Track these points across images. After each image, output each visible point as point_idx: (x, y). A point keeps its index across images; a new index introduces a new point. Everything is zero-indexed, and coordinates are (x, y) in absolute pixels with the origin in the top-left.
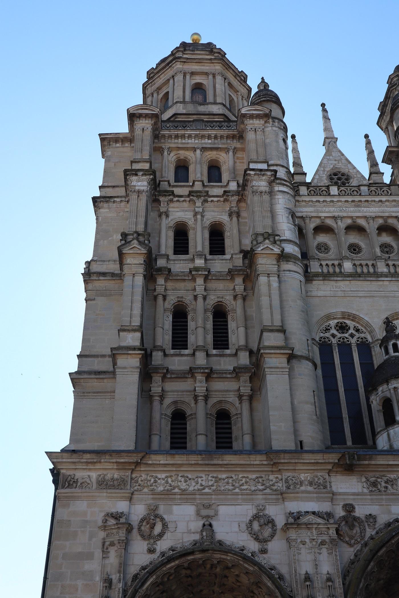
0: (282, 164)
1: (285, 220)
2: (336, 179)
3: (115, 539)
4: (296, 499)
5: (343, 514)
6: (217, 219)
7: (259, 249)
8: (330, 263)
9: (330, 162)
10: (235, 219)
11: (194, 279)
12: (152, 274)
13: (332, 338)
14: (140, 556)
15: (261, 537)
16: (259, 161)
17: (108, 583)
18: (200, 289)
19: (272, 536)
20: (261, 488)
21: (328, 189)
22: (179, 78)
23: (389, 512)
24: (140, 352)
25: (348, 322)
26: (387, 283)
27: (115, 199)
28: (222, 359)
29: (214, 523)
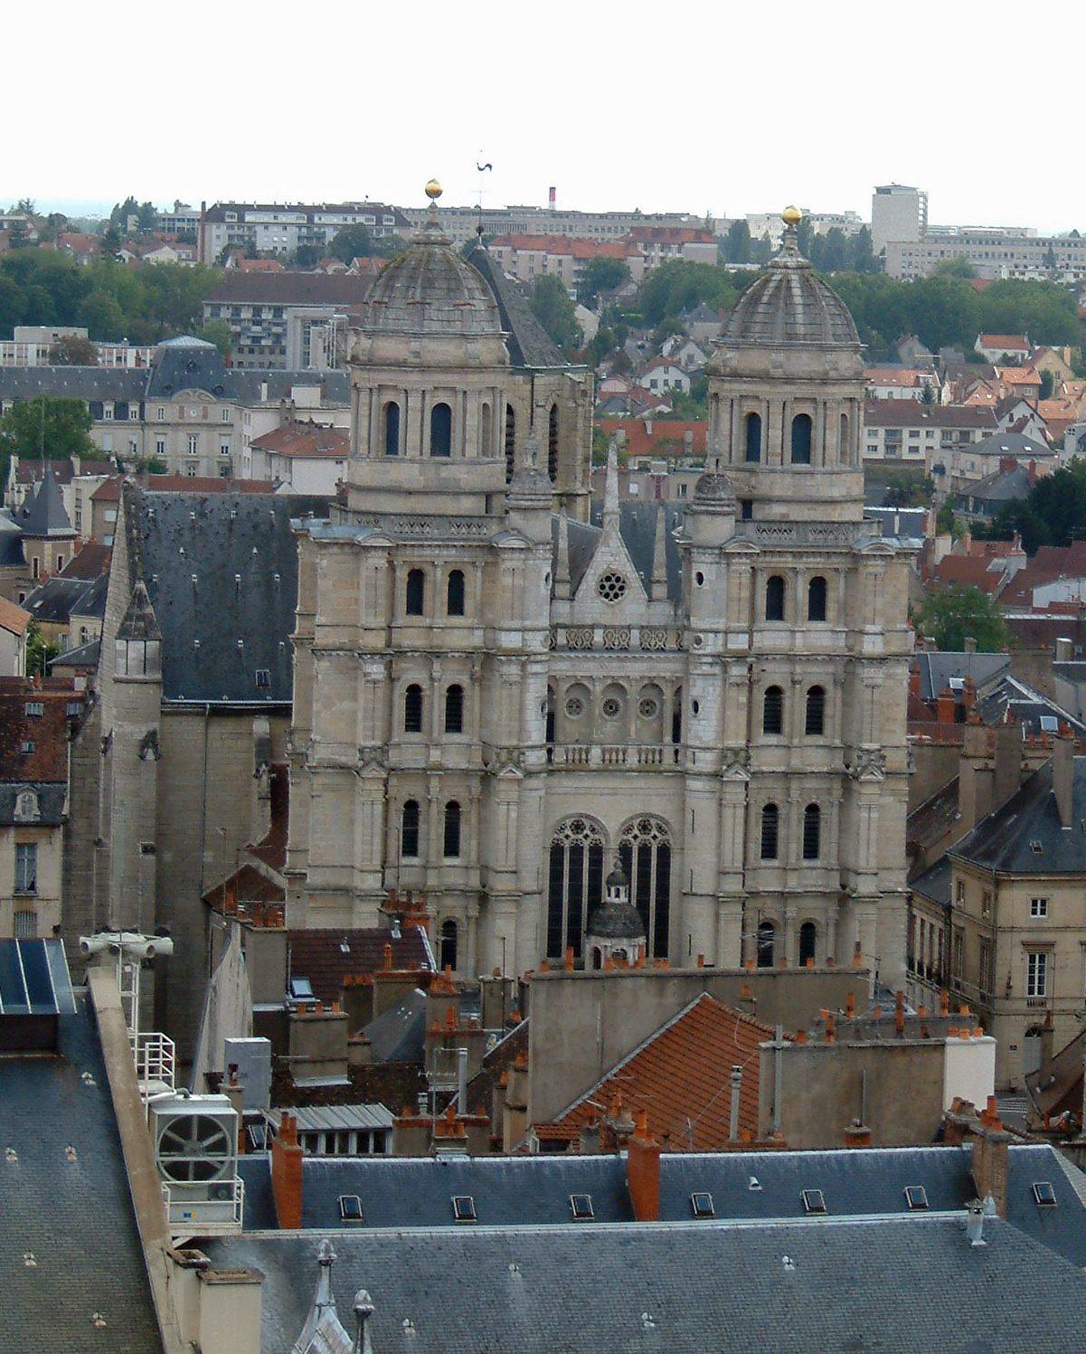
2: (607, 588)
11: (428, 777)
22: (414, 402)
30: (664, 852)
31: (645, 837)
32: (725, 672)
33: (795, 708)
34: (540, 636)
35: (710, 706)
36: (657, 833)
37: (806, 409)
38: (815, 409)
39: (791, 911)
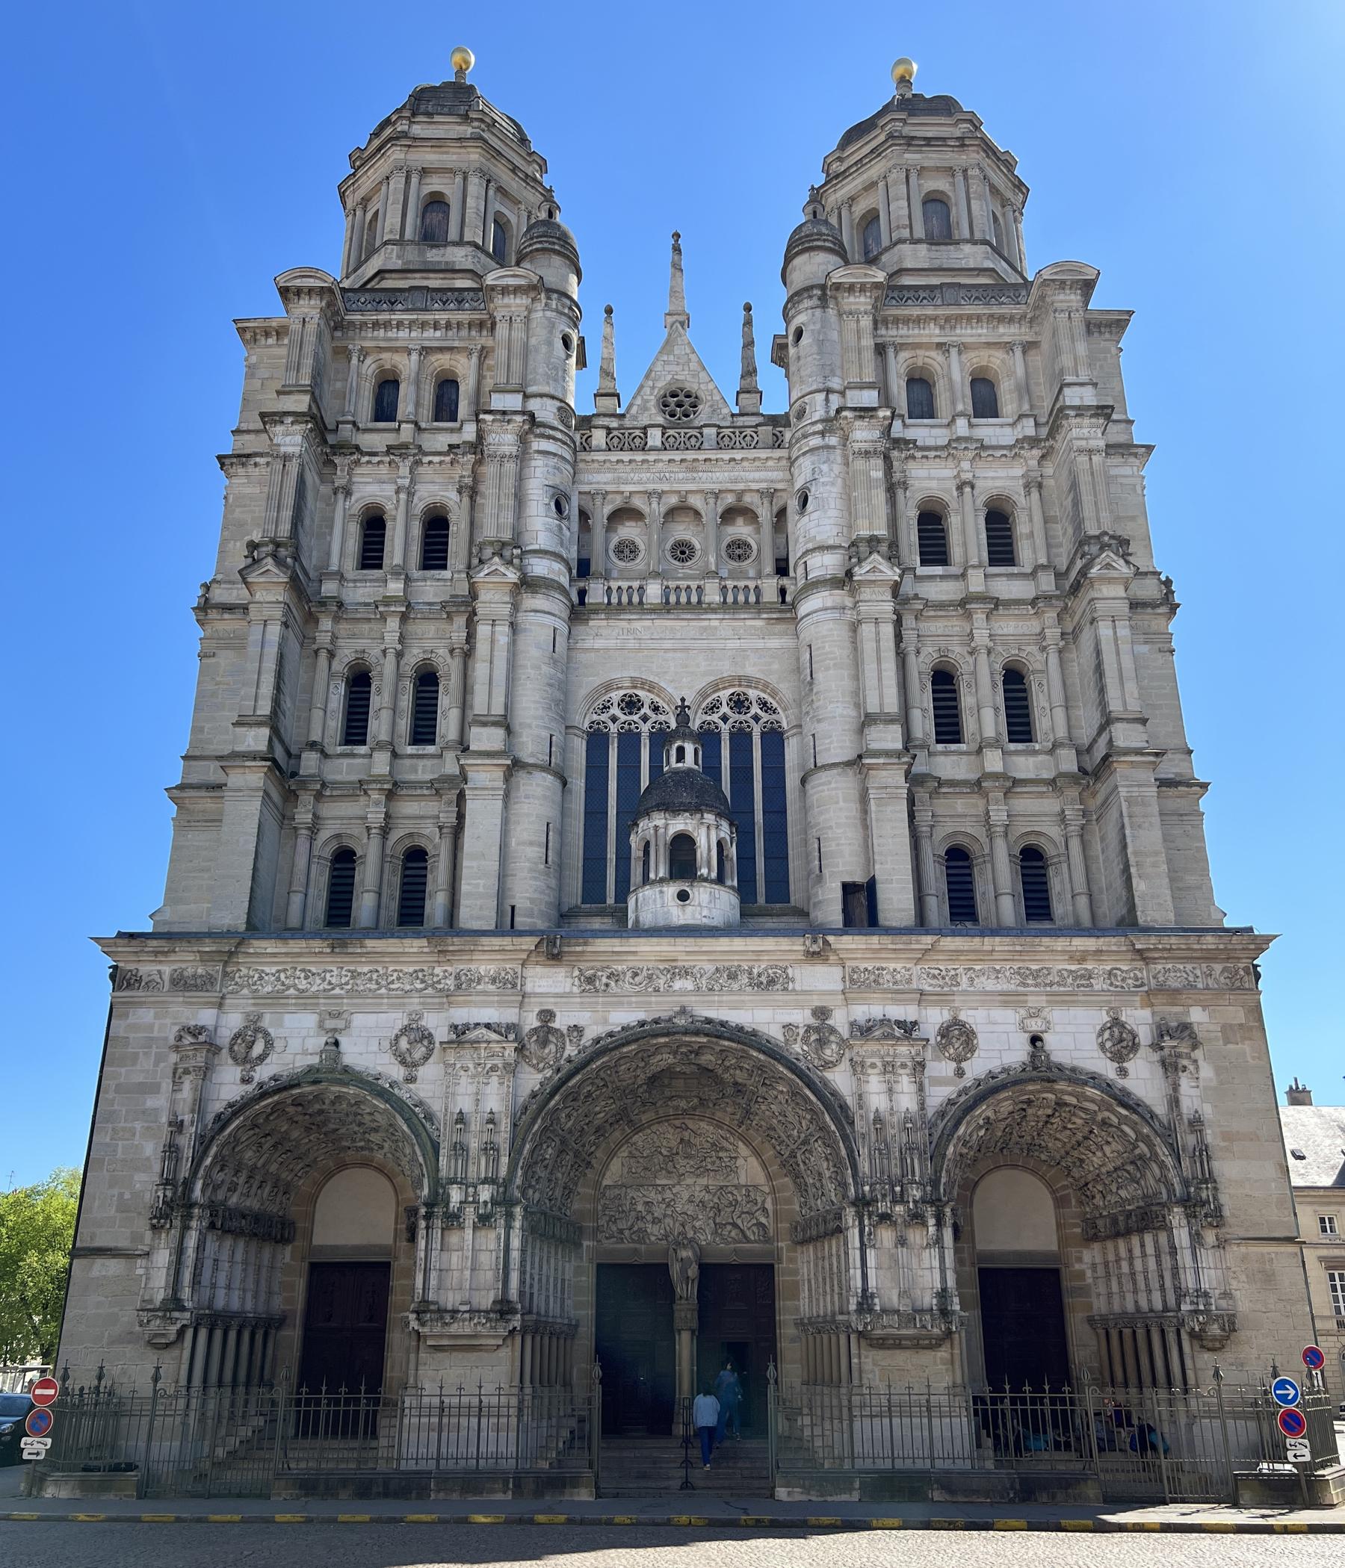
0: (552, 392)
1: (542, 510)
3: (190, 1064)
4: (466, 1004)
5: (536, 1024)
6: (437, 499)
7: (482, 574)
8: (625, 585)
9: (667, 368)
10: (466, 500)
11: (383, 618)
12: (310, 613)
13: (610, 724)
14: (229, 1085)
15: (409, 1060)
16: (509, 387)
17: (177, 1126)
18: (391, 638)
19: (426, 1058)
20: (419, 986)
21: (645, 434)
22: (397, 183)
23: (606, 1022)
24: (264, 763)
25: (640, 693)
26: (716, 623)
27: (258, 459)
28: (421, 763)
29: (342, 1040)
30: (774, 739)
31: (742, 717)
32: (845, 439)
33: (967, 534)
34: (552, 406)
35: (828, 494)
36: (759, 711)
37: (940, 184)
38: (953, 184)
39: (999, 815)
